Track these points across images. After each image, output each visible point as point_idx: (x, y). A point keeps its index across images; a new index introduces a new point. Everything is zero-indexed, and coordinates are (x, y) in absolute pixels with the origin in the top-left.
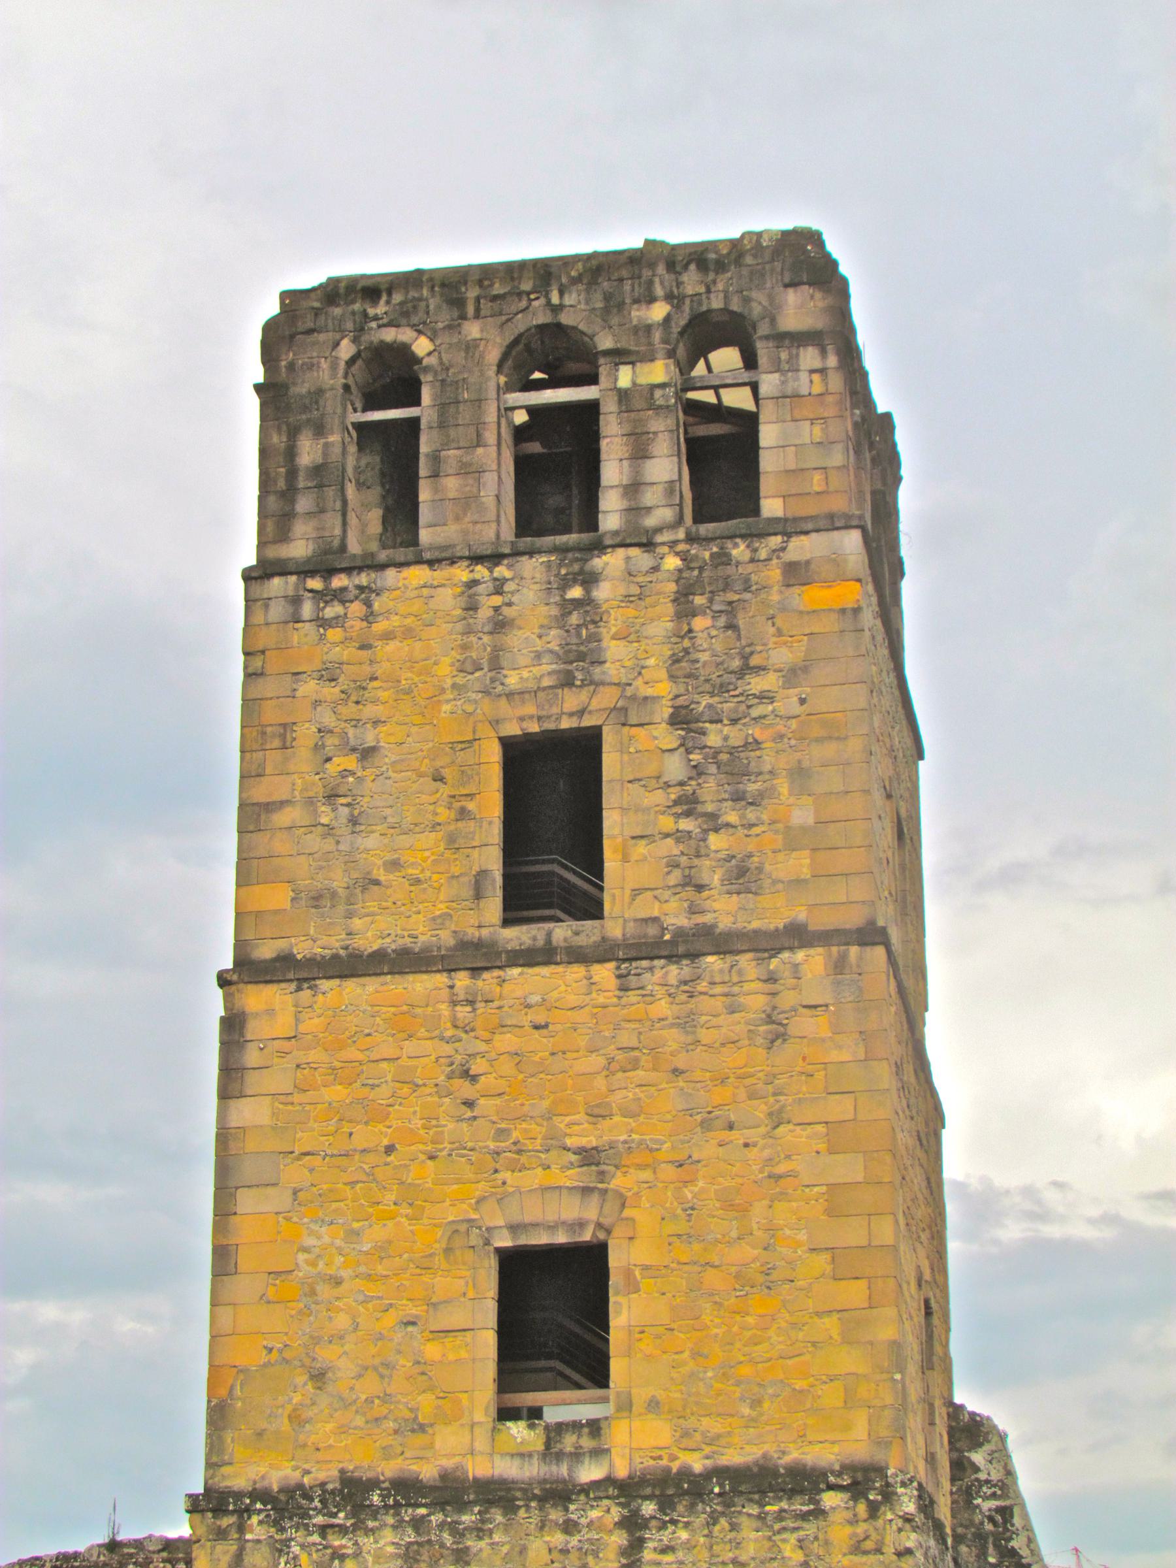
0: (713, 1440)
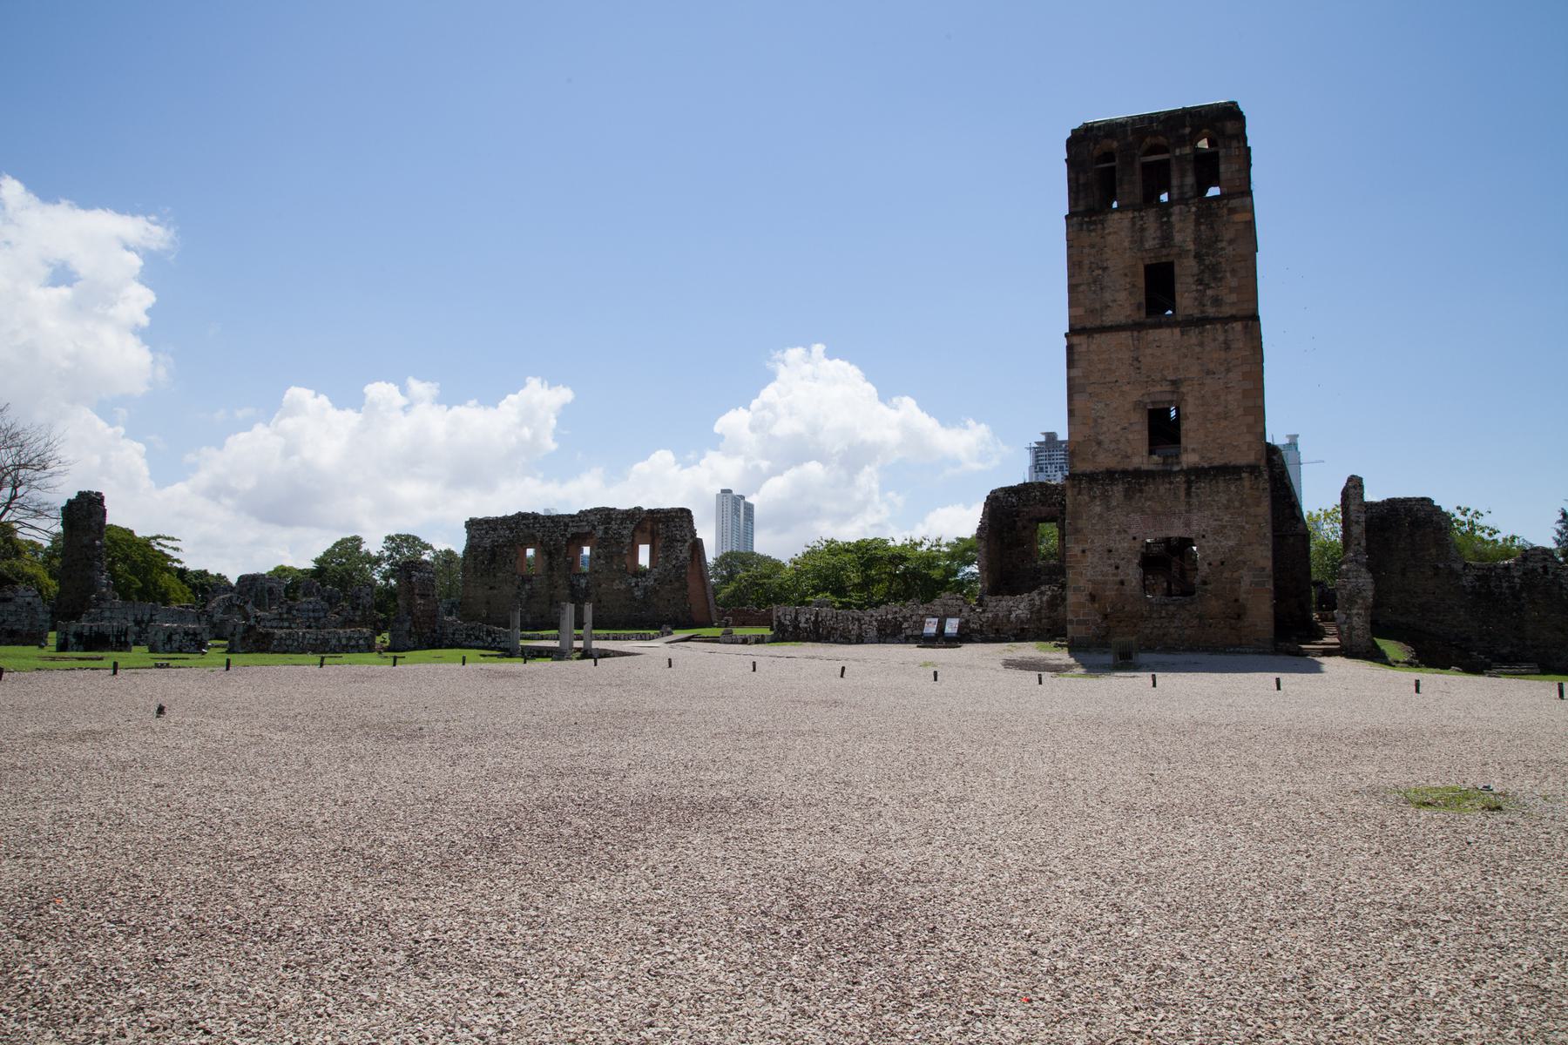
0: (1210, 459)
